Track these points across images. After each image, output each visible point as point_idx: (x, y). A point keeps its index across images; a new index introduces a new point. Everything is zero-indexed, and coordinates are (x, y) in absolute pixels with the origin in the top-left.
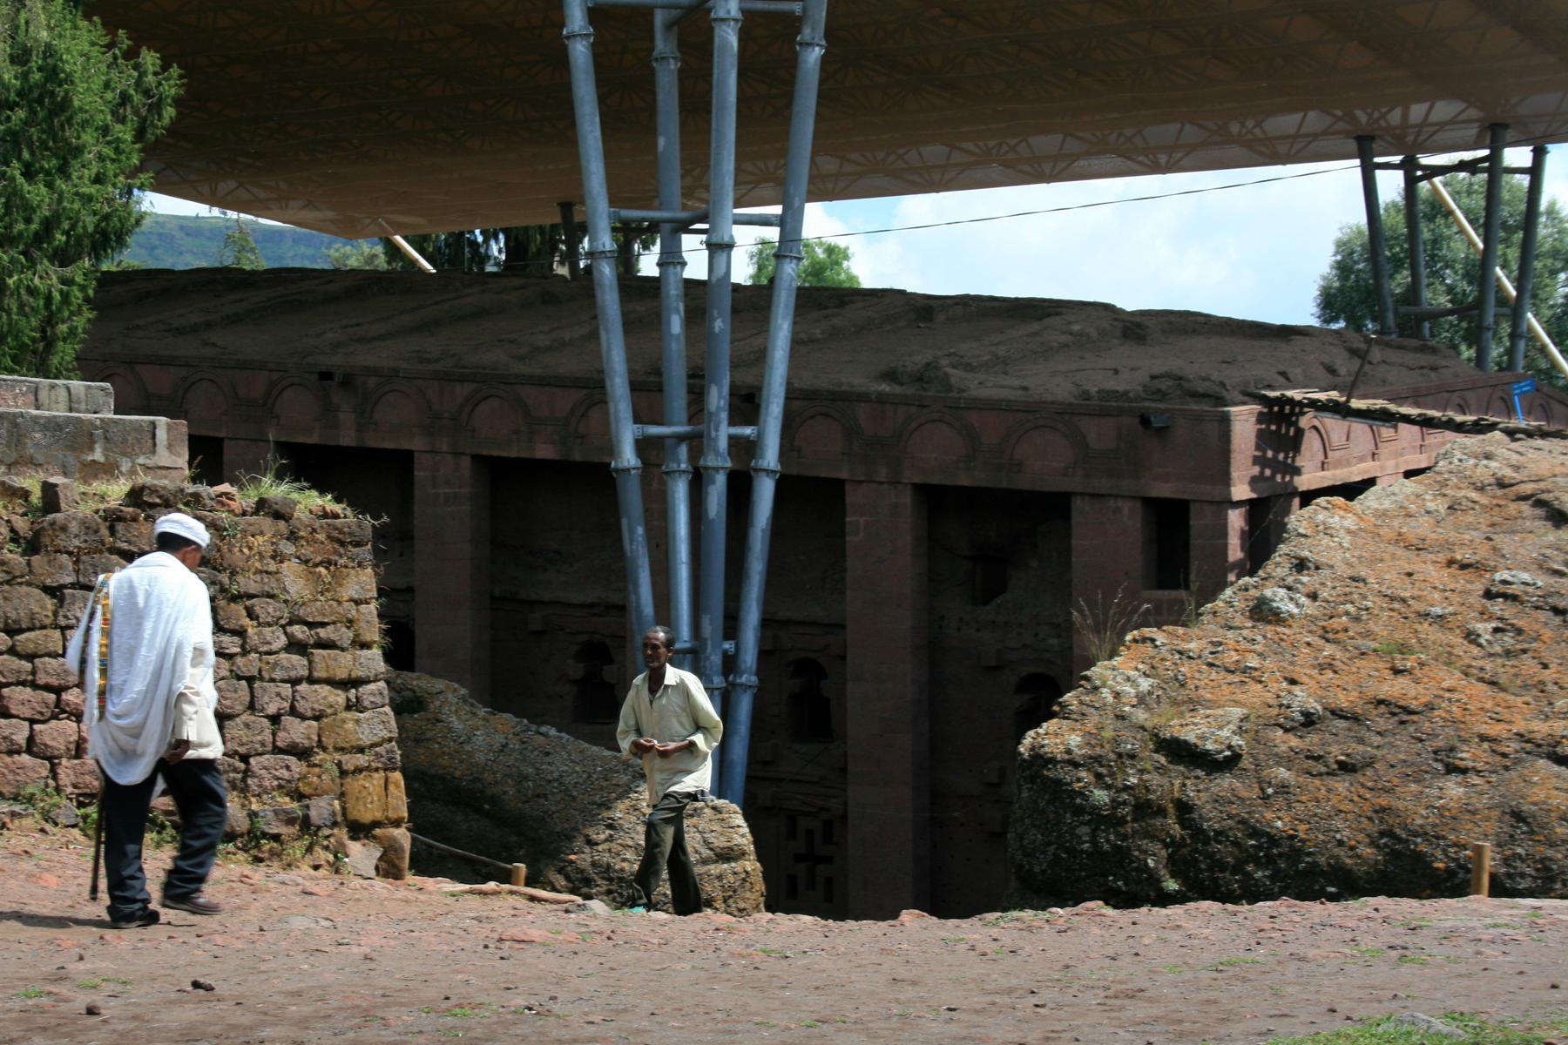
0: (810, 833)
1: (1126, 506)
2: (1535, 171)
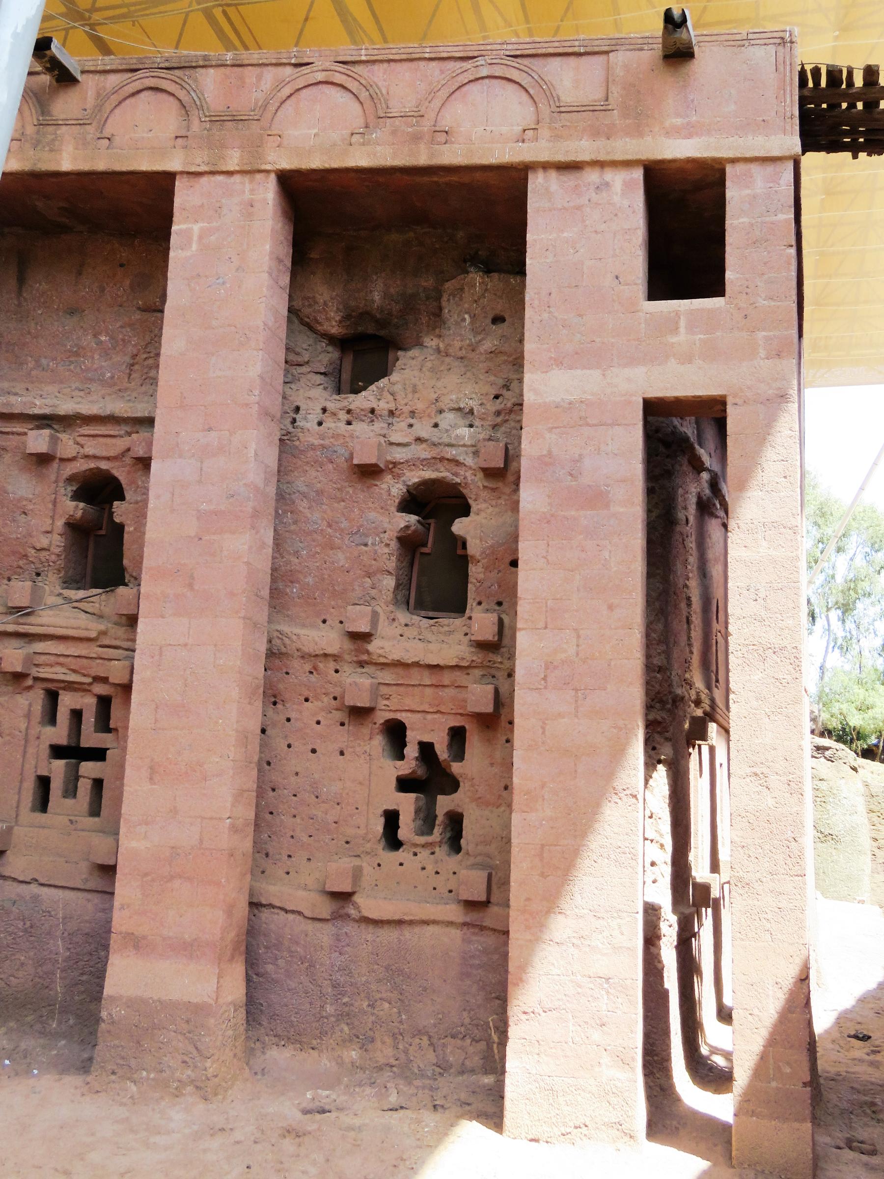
1: (617, 179)
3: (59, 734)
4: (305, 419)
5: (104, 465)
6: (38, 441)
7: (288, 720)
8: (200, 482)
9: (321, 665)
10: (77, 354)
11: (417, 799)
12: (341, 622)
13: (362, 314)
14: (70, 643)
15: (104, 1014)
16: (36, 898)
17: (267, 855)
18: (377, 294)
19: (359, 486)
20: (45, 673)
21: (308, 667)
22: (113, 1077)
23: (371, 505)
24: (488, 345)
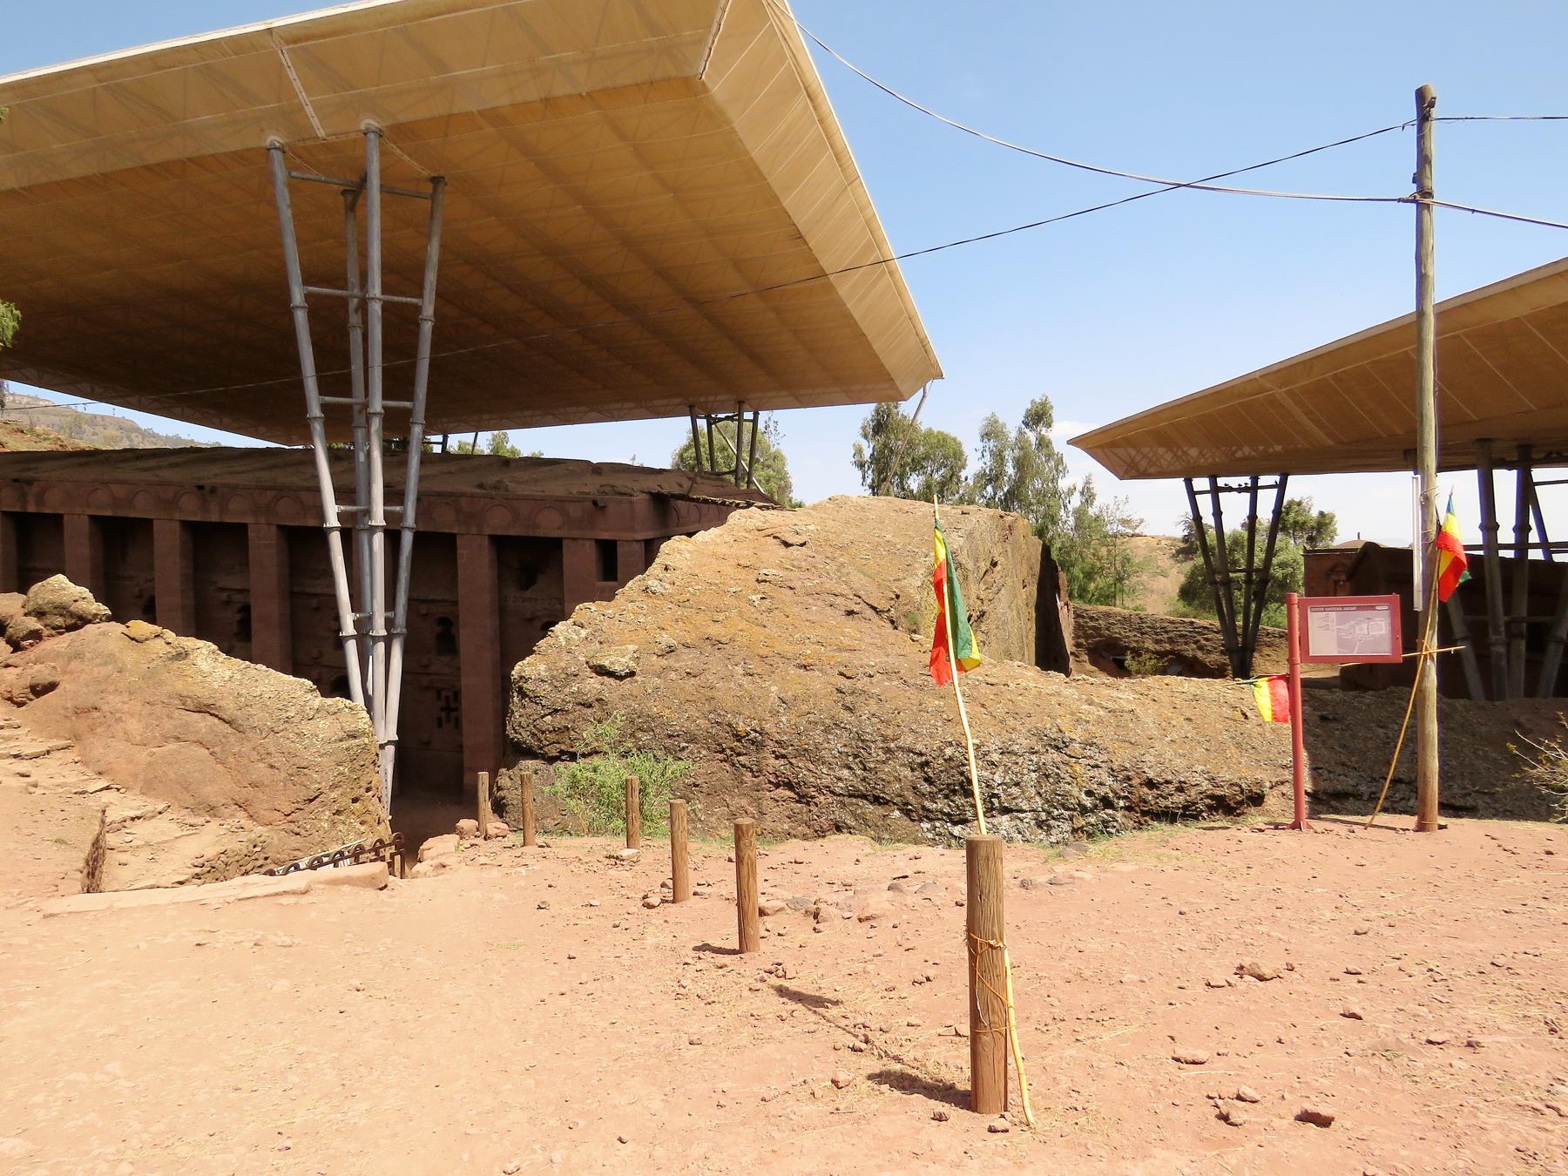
1: (587, 543)
2: (755, 421)
3: (442, 703)
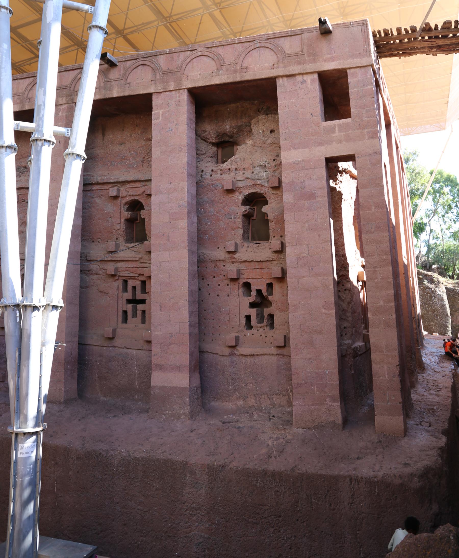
0: (134, 288)
3: (129, 295)
4: (206, 174)
5: (136, 198)
6: (113, 192)
7: (208, 285)
8: (169, 202)
9: (218, 264)
10: (124, 159)
11: (257, 310)
12: (224, 248)
13: (223, 134)
14: (130, 262)
15: (152, 392)
16: (126, 353)
17: (205, 334)
18: (228, 126)
19: (227, 197)
20: (122, 274)
21: (214, 265)
22: (157, 414)
23: (231, 204)
24: (269, 141)
